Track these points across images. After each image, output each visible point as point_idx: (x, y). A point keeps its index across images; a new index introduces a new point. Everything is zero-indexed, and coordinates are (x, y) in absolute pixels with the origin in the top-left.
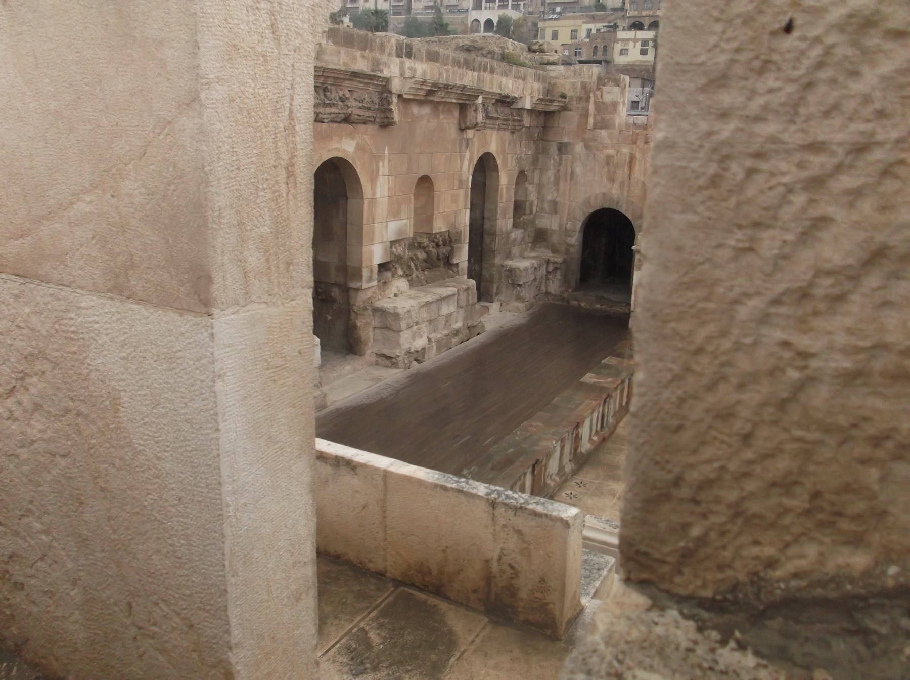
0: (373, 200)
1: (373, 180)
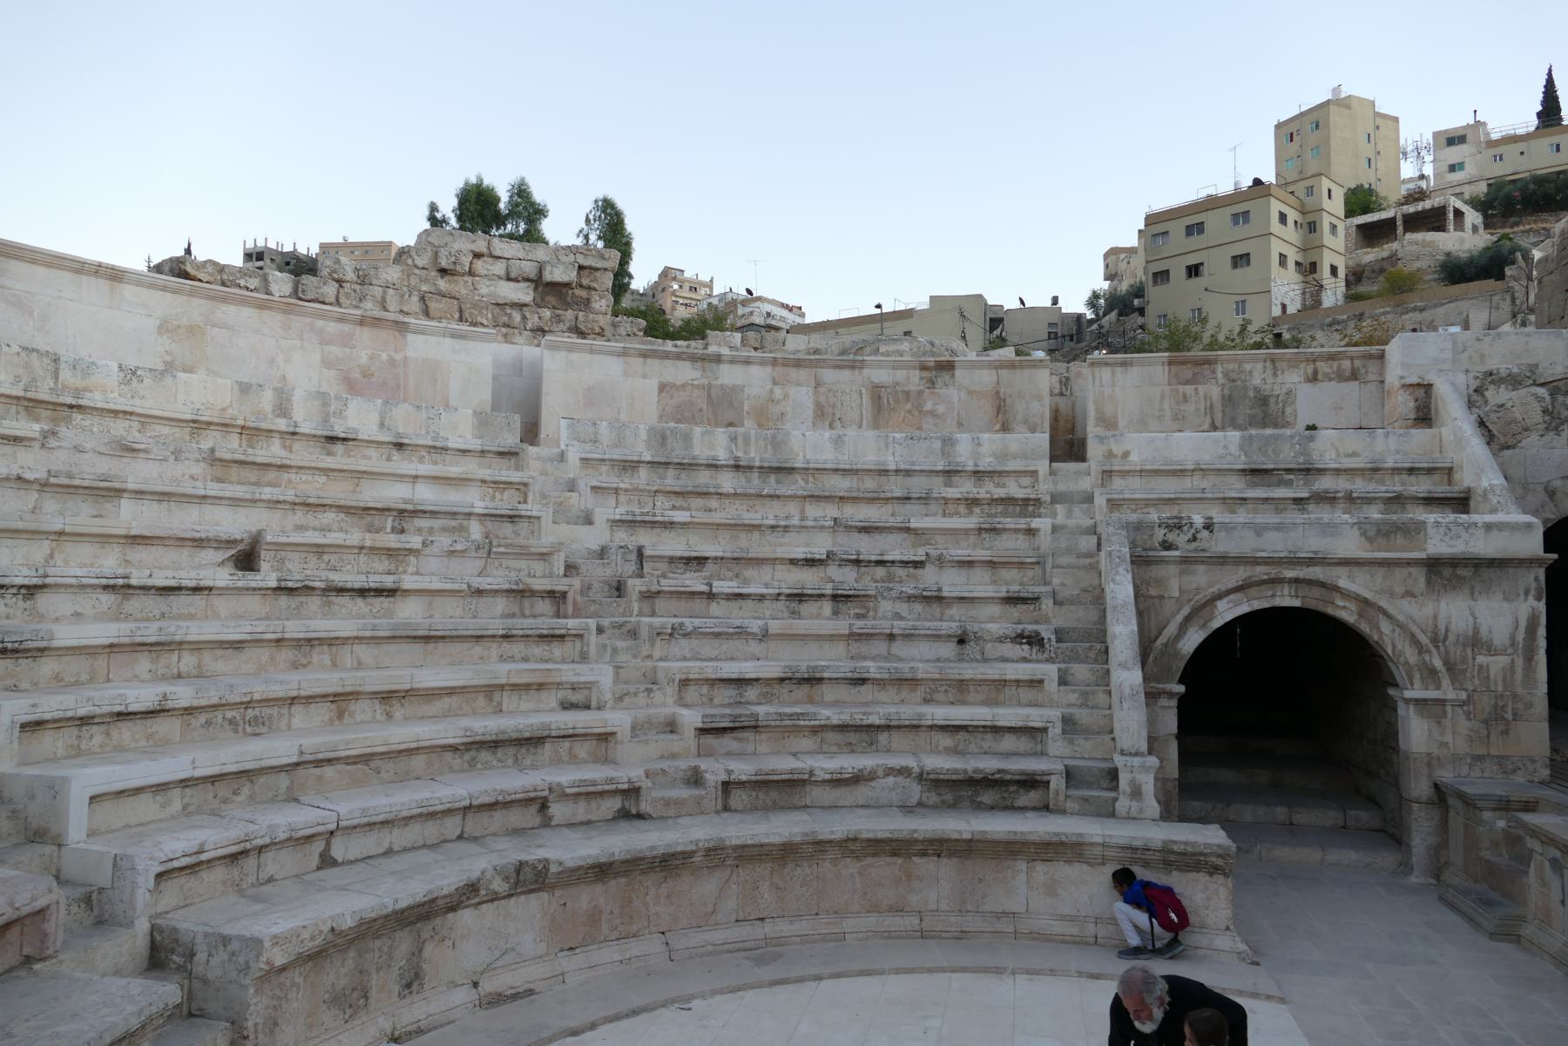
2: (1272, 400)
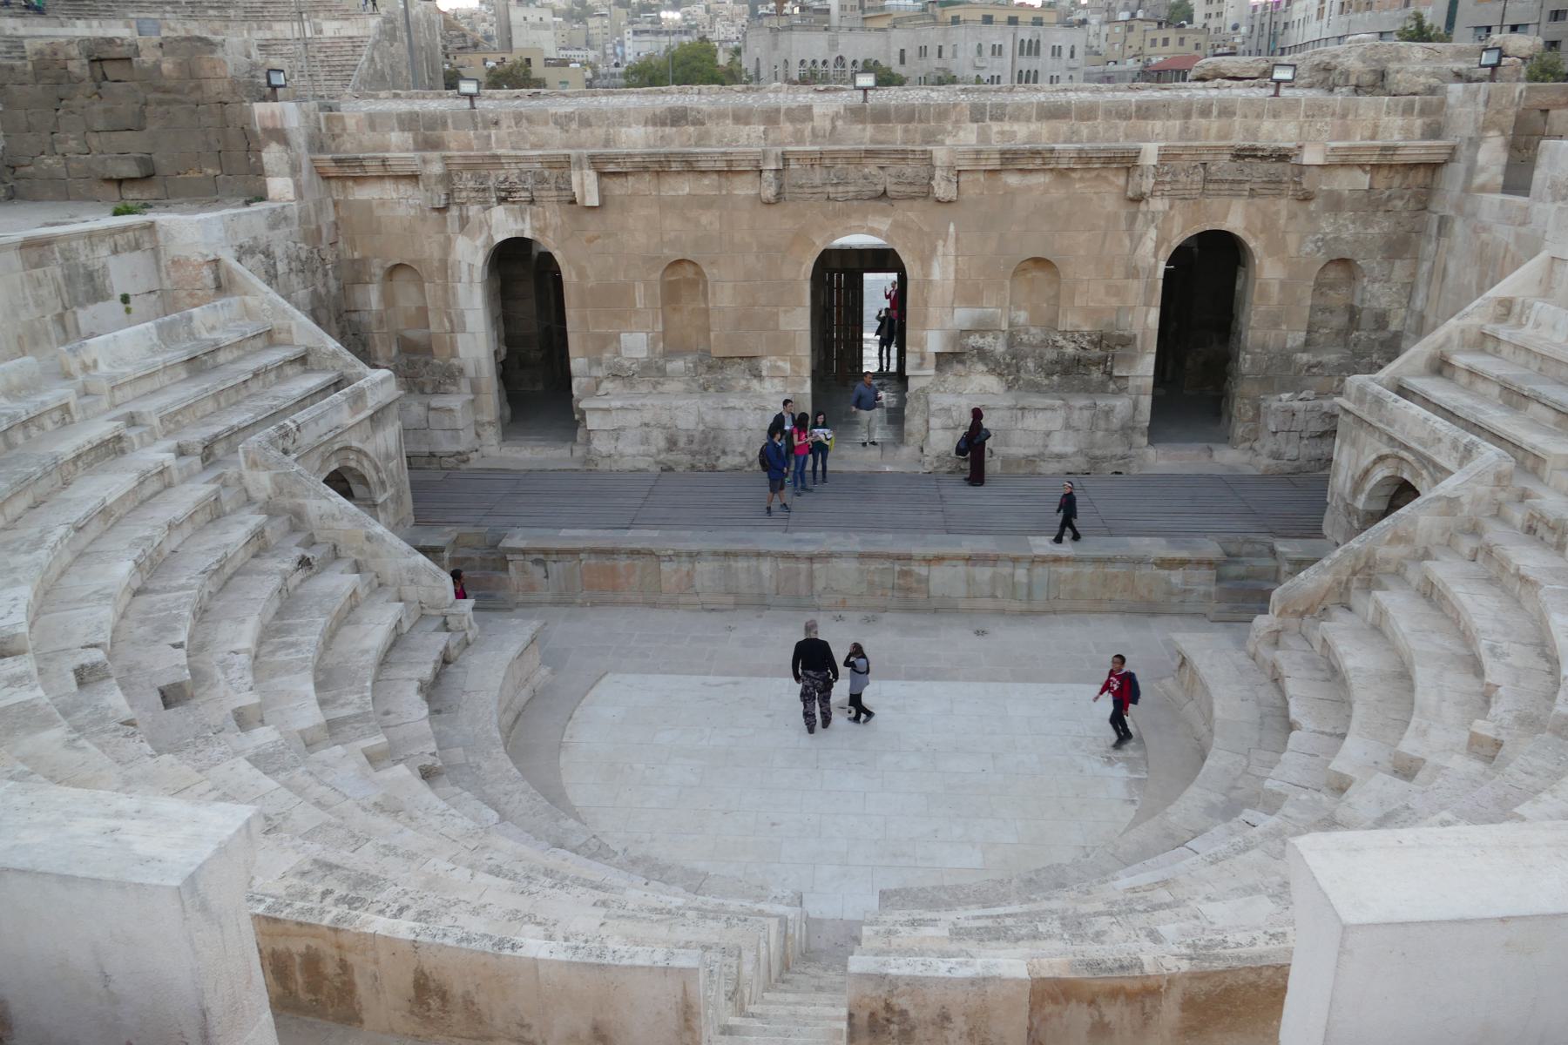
0: (927, 282)
1: (926, 261)
2: (95, 274)
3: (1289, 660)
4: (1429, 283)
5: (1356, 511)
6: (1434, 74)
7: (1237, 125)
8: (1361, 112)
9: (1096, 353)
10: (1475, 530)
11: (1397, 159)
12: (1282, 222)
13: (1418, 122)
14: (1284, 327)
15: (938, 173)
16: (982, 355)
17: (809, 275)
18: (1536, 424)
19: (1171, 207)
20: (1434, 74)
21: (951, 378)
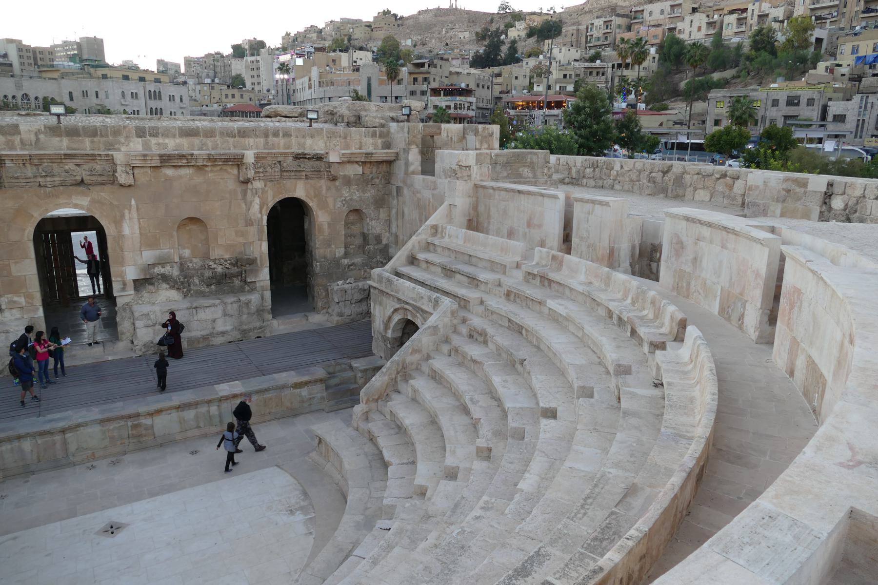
0: (120, 236)
3: (376, 426)
4: (397, 219)
5: (388, 338)
6: (382, 118)
7: (293, 141)
8: (353, 135)
9: (235, 270)
10: (447, 341)
11: (373, 159)
12: (324, 192)
13: (380, 141)
14: (333, 246)
15: (119, 169)
16: (165, 278)
17: (32, 237)
18: (460, 283)
19: (265, 186)
20: (382, 118)
21: (145, 294)
